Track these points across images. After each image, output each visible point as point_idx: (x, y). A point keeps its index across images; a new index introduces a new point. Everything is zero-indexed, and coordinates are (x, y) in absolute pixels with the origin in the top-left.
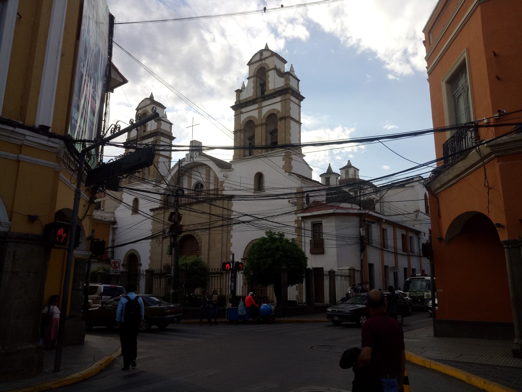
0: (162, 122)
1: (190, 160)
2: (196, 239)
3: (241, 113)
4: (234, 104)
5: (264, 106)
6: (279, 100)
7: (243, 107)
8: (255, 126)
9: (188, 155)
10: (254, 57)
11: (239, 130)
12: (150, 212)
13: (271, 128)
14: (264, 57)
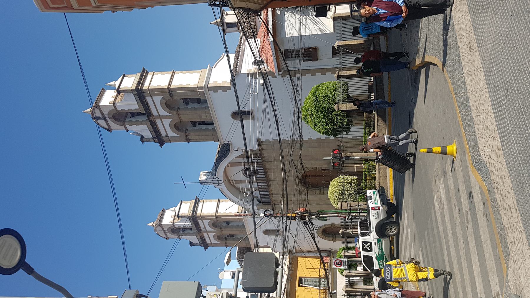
1: (222, 183)
3: (167, 136)
4: (158, 144)
5: (158, 113)
6: (151, 98)
7: (161, 135)
8: (181, 122)
13: (182, 105)
14: (101, 116)
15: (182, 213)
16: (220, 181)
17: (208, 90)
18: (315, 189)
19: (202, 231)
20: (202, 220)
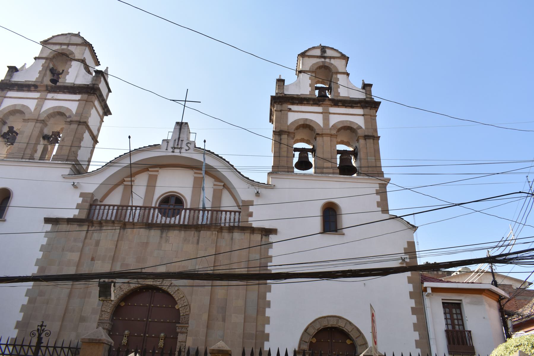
0: (102, 79)
2: (174, 299)
3: (290, 110)
7: (293, 104)
9: (168, 142)
10: (309, 49)
11: (286, 132)
12: (44, 224)
14: (326, 55)
15: (101, 80)
16: (180, 152)
17: (379, 184)
18: (113, 313)
19: (48, 93)
20: (79, 100)
